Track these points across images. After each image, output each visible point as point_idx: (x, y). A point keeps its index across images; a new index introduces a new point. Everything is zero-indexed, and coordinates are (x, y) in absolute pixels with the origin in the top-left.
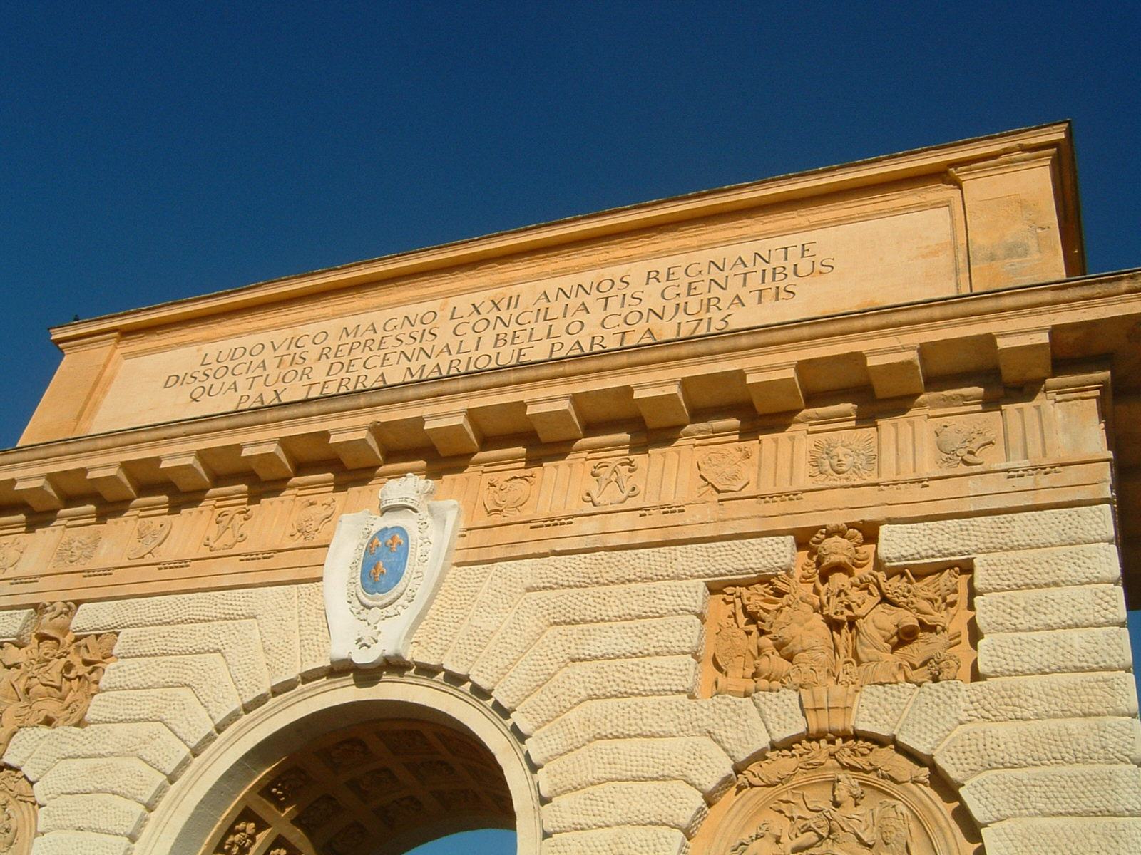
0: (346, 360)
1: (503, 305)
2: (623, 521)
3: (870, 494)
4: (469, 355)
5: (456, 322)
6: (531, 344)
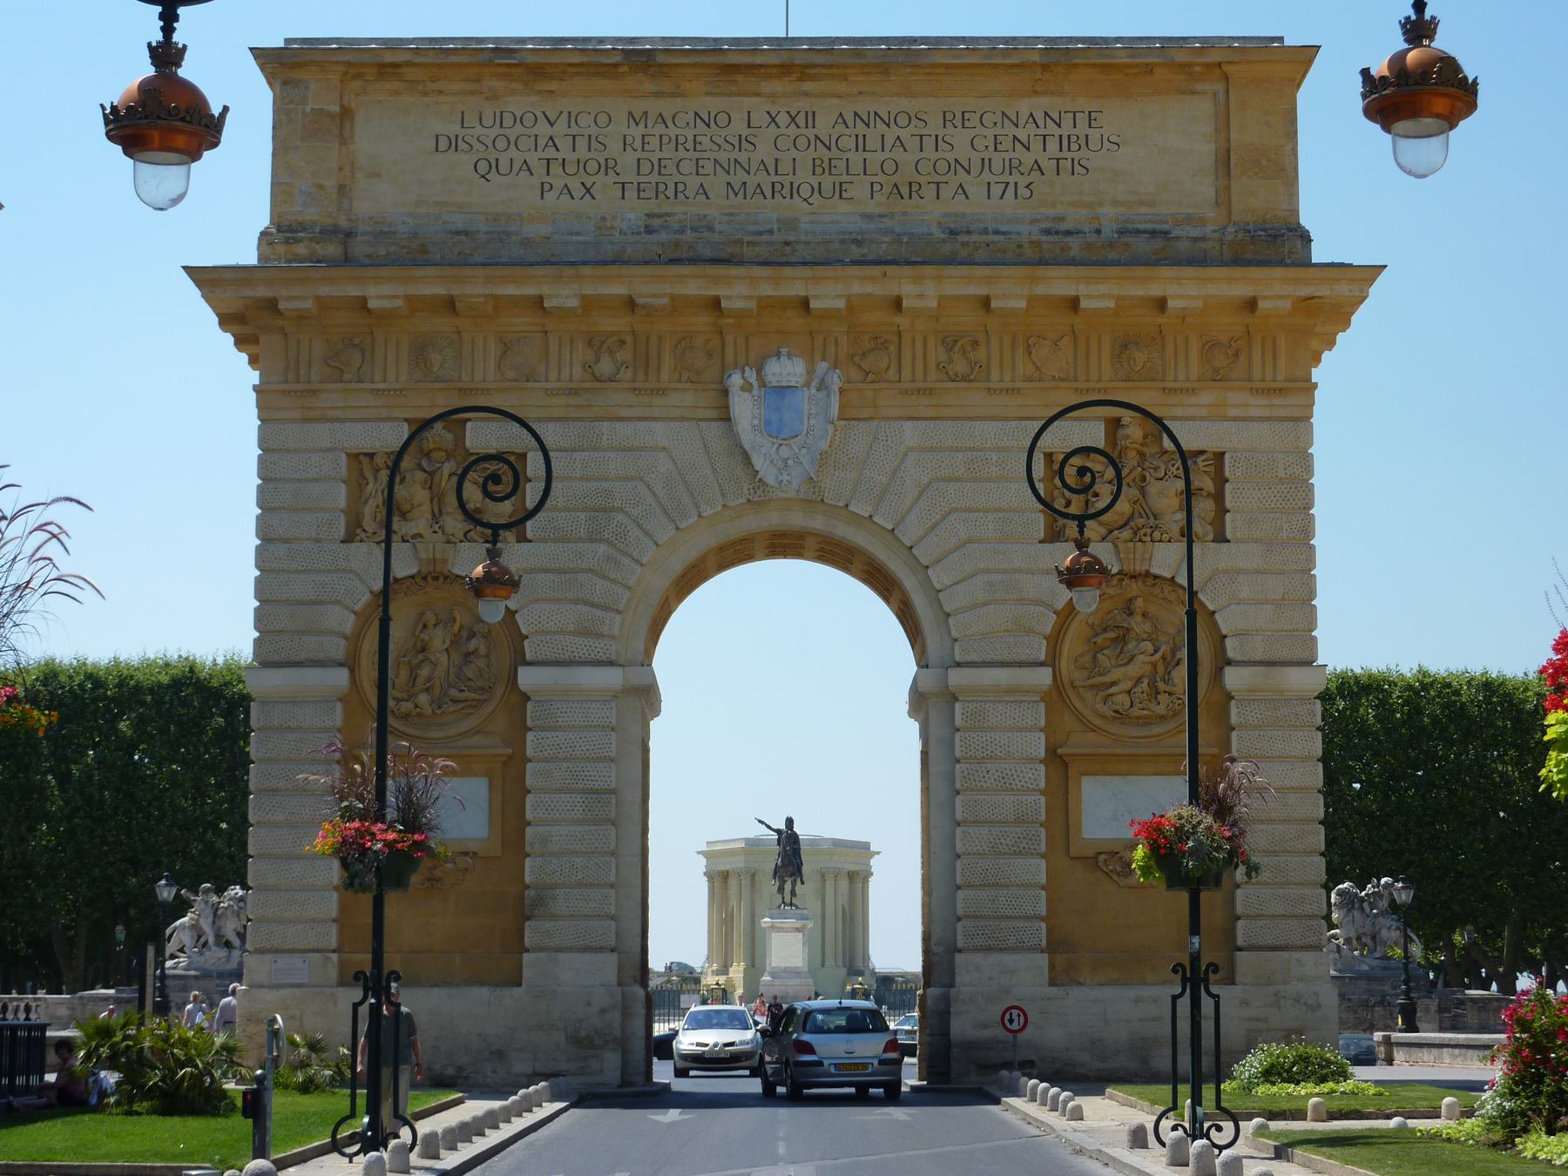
0: (654, 158)
4: (790, 178)
6: (849, 178)
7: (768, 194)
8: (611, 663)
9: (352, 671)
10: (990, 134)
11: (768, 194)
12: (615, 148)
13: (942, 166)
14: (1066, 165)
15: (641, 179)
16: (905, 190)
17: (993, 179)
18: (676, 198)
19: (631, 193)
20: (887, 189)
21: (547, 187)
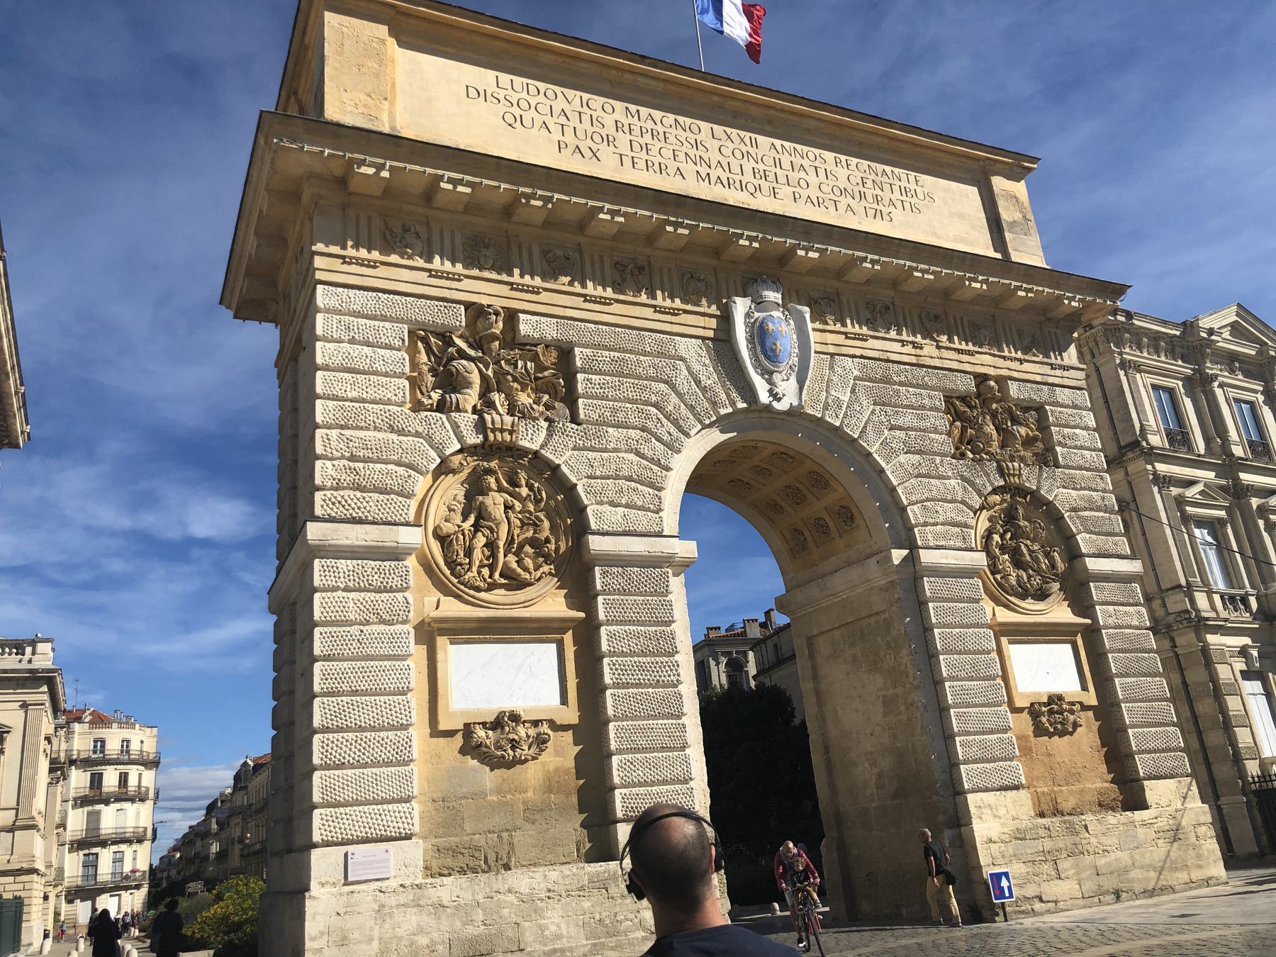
5: (717, 144)
6: (779, 186)
12: (610, 129)
13: (837, 191)
14: (907, 205)
15: (633, 154)
17: (868, 205)
18: (661, 173)
19: (627, 161)
20: (804, 197)
21: (563, 145)
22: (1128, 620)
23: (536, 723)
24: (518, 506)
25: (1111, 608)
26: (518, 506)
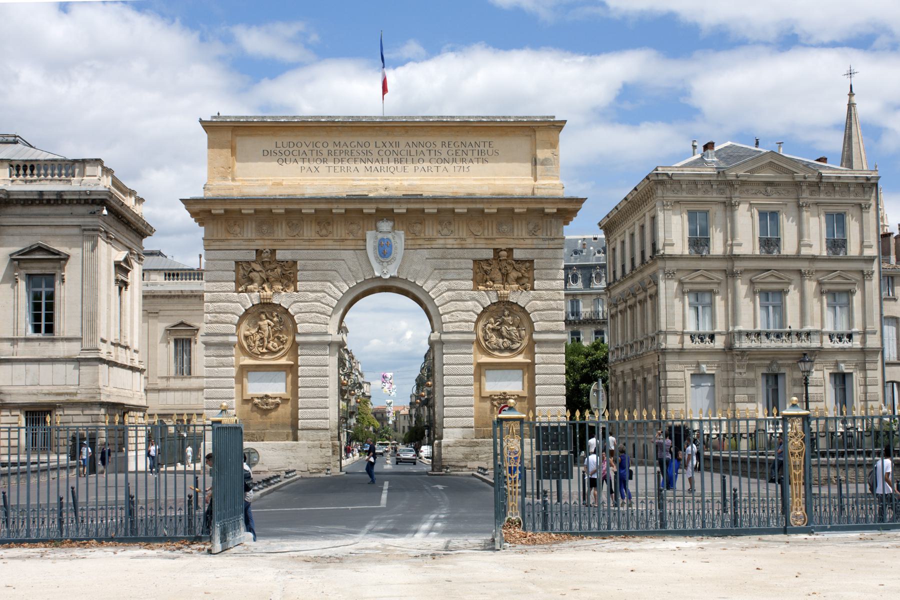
1: (394, 145)
2: (450, 241)
3: (512, 241)
5: (378, 149)
7: (379, 170)
8: (326, 334)
9: (238, 336)
10: (454, 149)
11: (379, 170)
16: (426, 169)
20: (420, 168)
22: (553, 361)
23: (275, 398)
24: (272, 324)
25: (545, 355)
26: (272, 324)
